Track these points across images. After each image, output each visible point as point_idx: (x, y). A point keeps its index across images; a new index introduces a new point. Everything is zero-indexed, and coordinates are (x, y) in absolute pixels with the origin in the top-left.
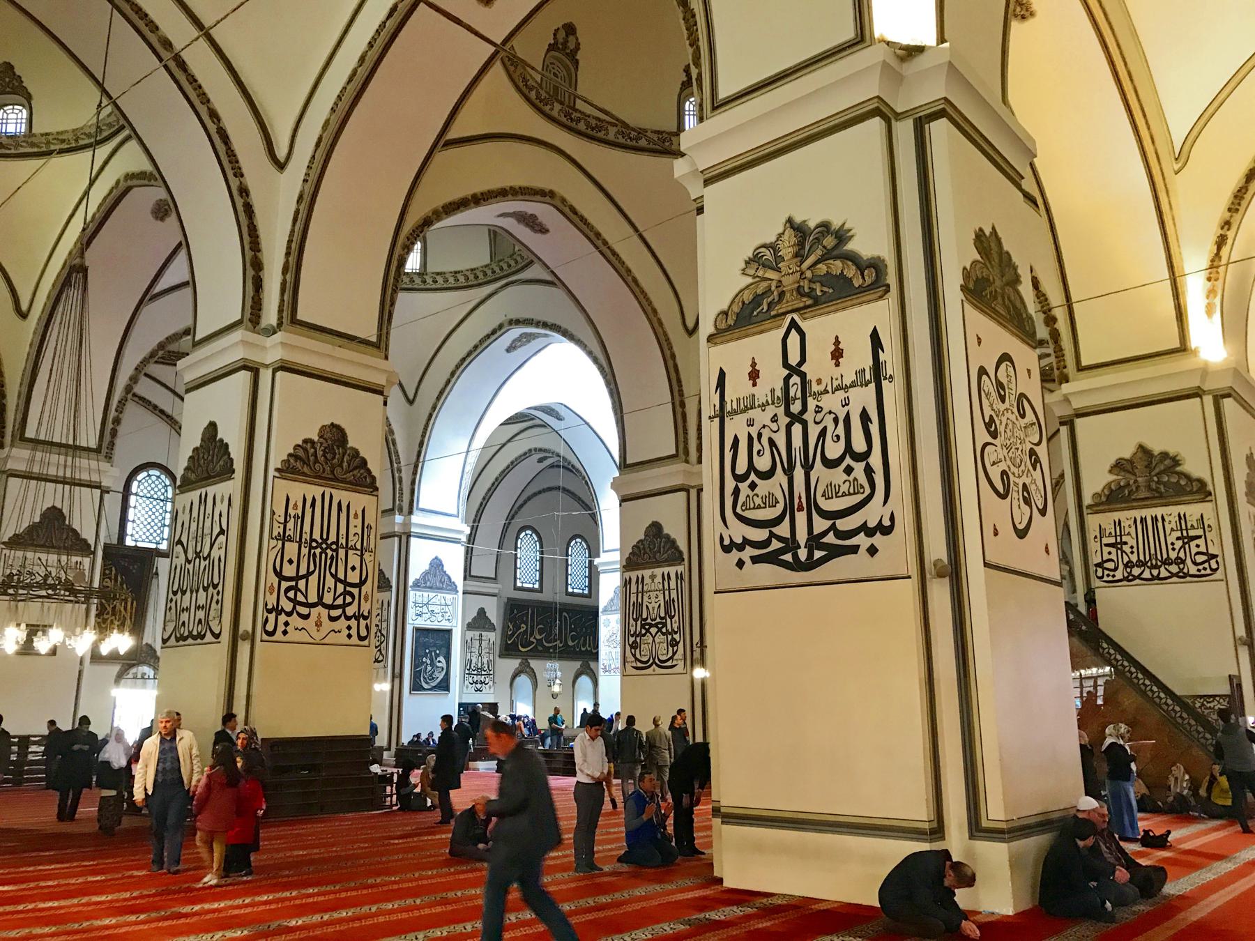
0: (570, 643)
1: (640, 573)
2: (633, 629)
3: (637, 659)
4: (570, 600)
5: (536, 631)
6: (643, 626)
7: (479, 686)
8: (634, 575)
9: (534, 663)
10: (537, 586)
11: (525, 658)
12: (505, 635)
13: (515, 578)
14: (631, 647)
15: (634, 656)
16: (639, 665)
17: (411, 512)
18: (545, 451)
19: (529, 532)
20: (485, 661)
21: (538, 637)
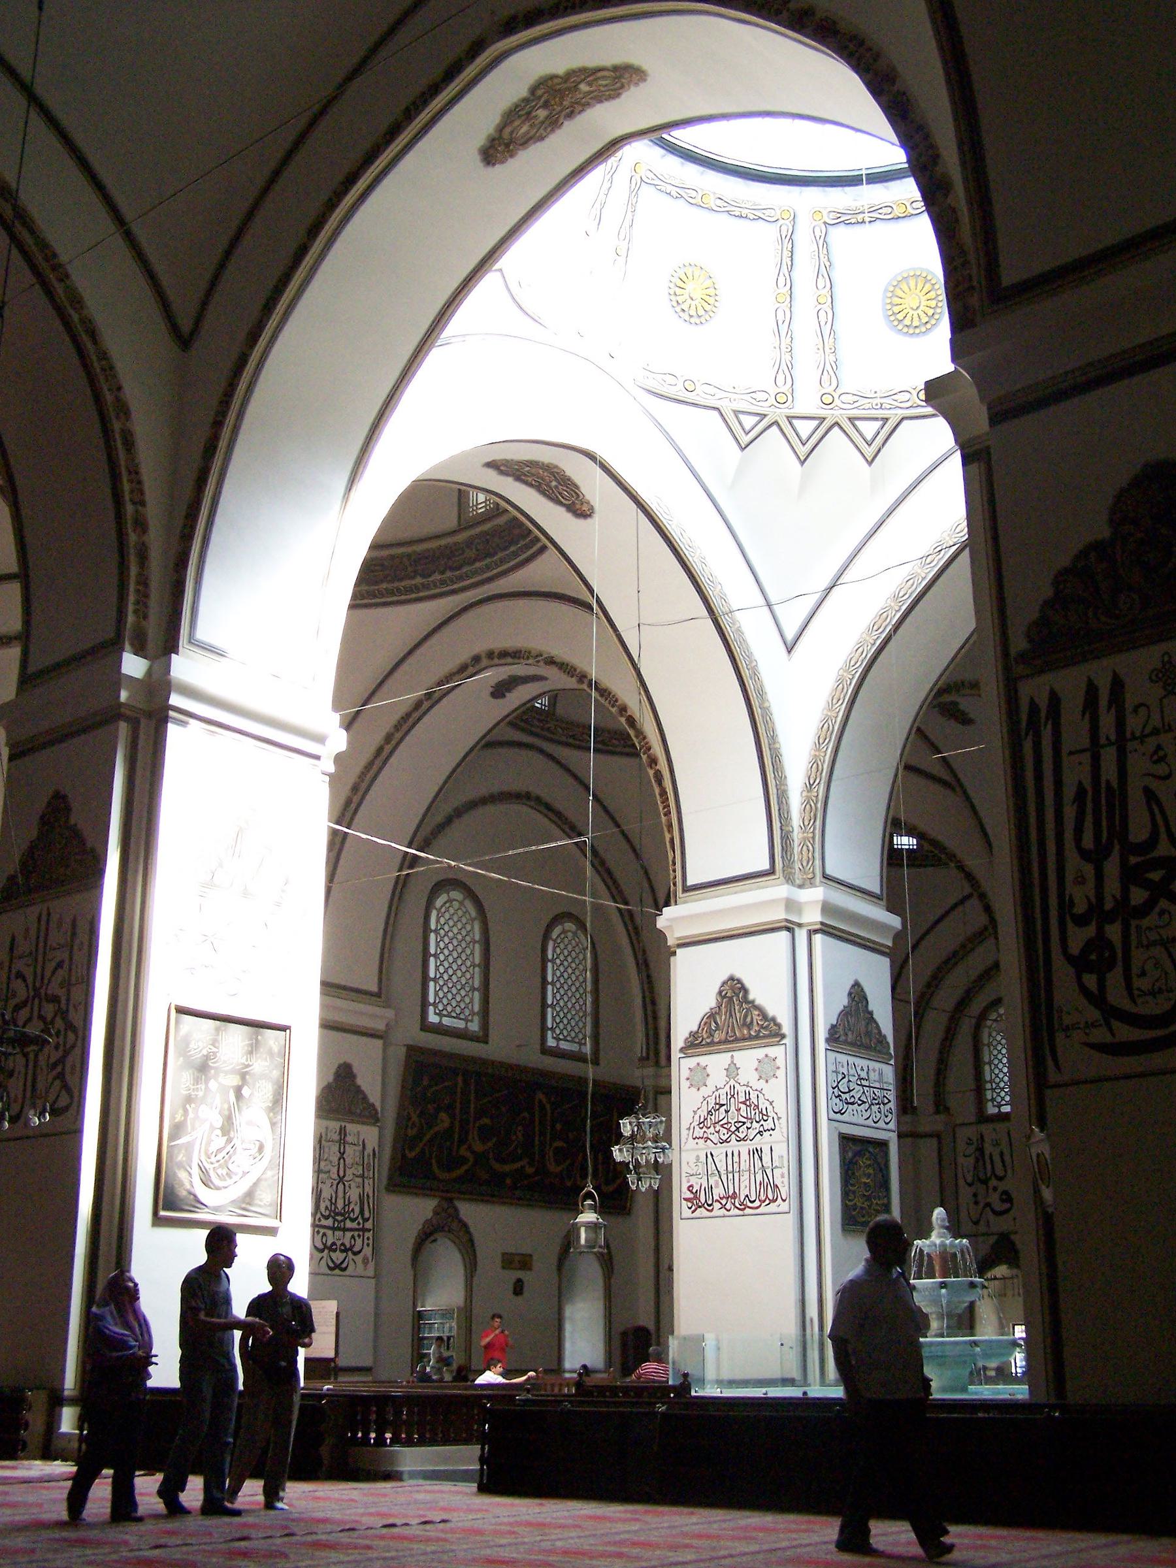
0: (553, 1168)
1: (1100, 671)
2: (1081, 897)
3: (1112, 1013)
4: (549, 1063)
5: (473, 1135)
6: (1130, 876)
7: (338, 1256)
8: (1068, 683)
9: (469, 1211)
10: (474, 1026)
11: (448, 1194)
12: (404, 1140)
13: (424, 1004)
14: (1080, 964)
15: (1098, 999)
16: (1126, 1033)
17: (170, 646)
18: (516, 655)
19: (456, 895)
20: (354, 1193)
21: (478, 1147)
